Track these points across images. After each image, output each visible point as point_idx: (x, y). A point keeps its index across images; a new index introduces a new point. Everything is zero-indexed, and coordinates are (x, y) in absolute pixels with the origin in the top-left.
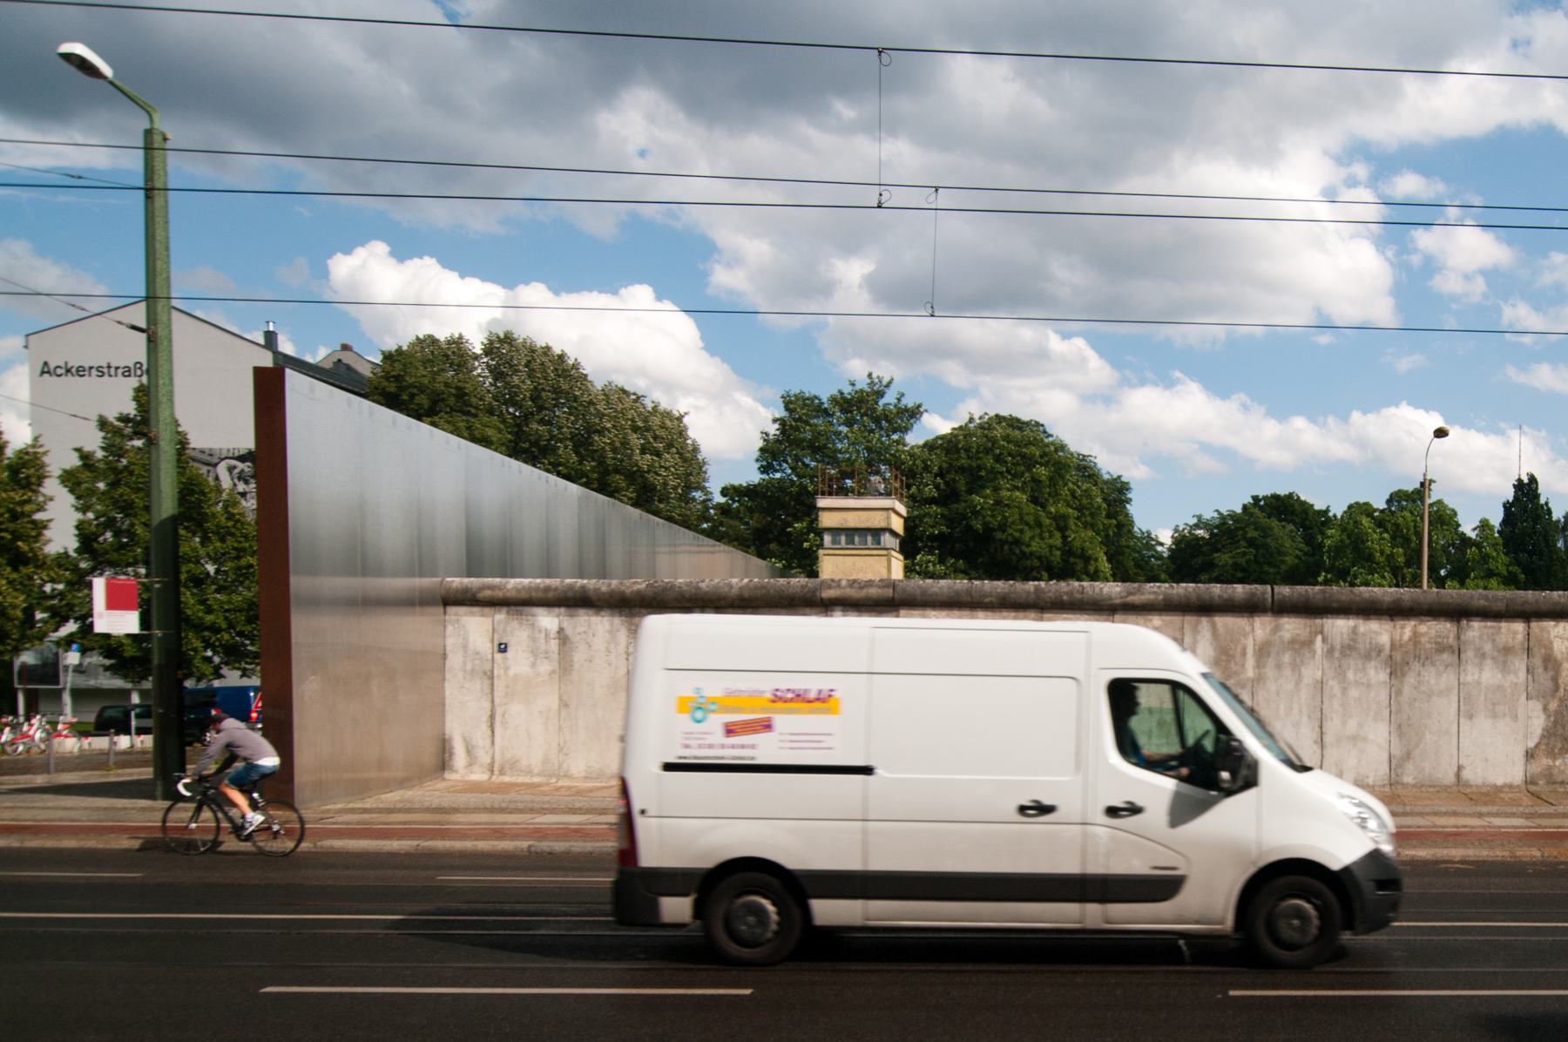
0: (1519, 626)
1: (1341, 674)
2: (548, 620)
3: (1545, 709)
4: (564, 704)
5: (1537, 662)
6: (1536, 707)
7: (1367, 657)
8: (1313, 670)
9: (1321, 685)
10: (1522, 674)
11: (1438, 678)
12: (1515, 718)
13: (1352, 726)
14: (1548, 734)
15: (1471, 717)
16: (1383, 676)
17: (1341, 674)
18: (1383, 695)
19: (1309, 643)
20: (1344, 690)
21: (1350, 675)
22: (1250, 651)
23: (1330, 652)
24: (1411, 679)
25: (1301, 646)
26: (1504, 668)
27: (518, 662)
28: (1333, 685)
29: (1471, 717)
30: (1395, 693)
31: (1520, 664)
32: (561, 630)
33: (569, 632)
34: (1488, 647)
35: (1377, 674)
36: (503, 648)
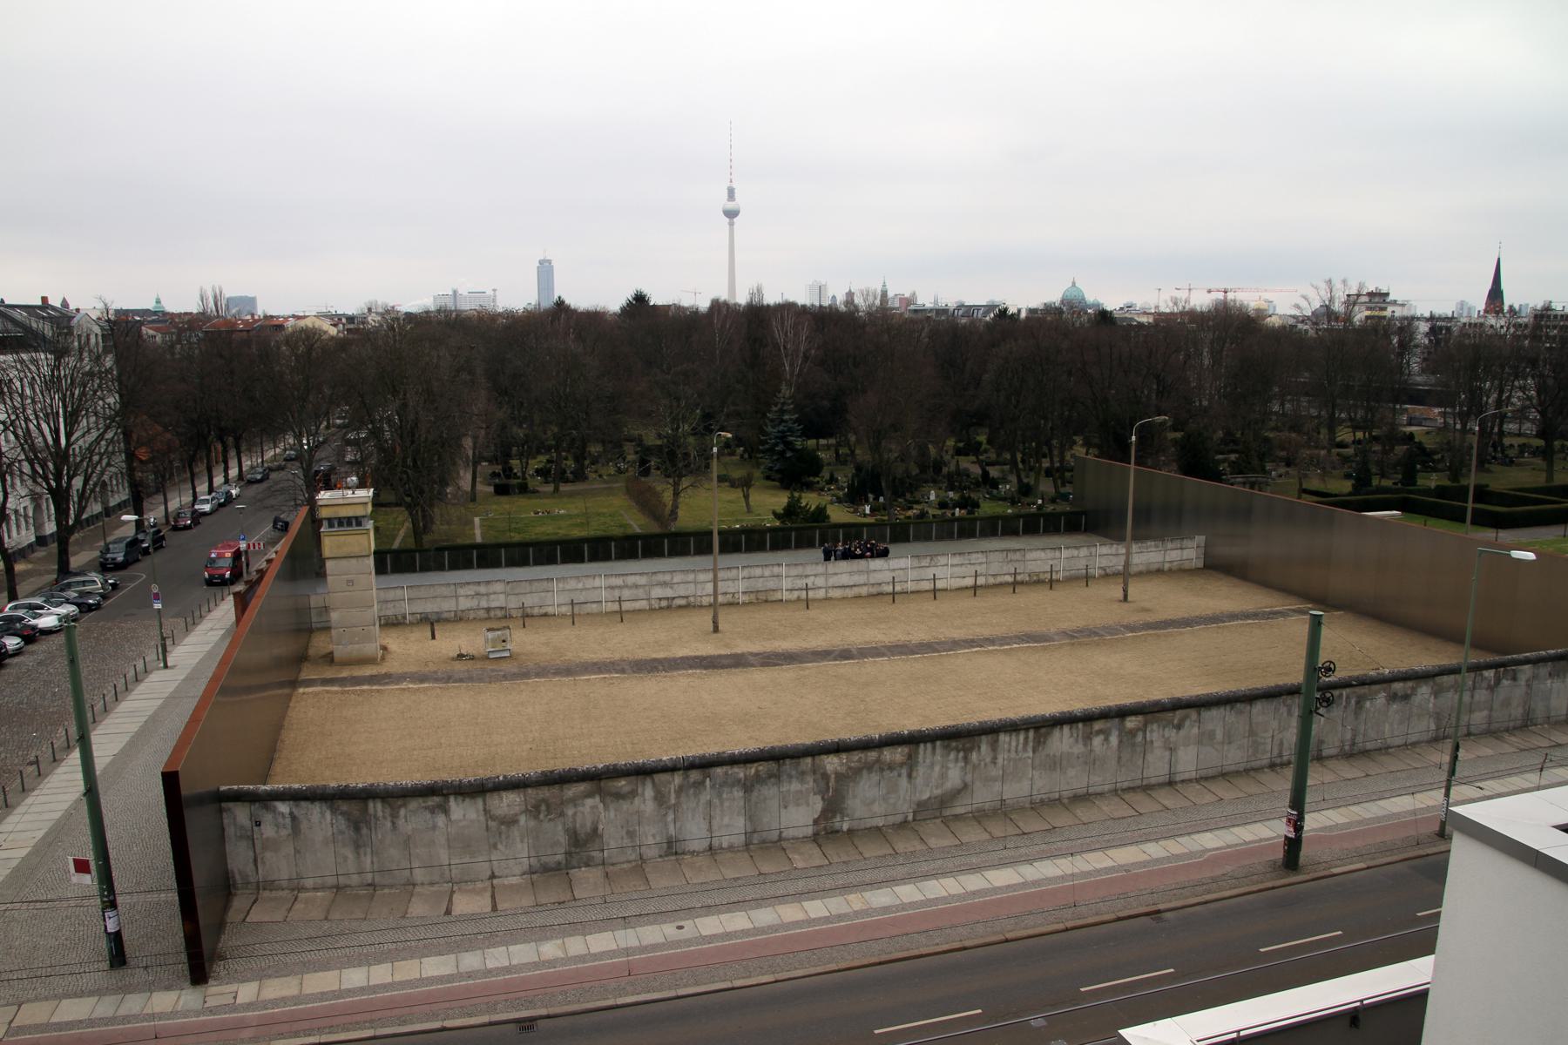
0: (809, 760)
1: (720, 795)
2: (283, 807)
4: (297, 851)
5: (818, 776)
7: (733, 785)
8: (706, 796)
9: (710, 803)
11: (769, 791)
13: (726, 820)
14: (824, 811)
16: (741, 794)
17: (720, 795)
19: (703, 782)
23: (713, 787)
24: (755, 794)
25: (699, 785)
26: (802, 781)
27: (268, 830)
28: (716, 801)
30: (747, 800)
31: (810, 779)
32: (291, 813)
33: (296, 812)
35: (738, 793)
36: (258, 824)
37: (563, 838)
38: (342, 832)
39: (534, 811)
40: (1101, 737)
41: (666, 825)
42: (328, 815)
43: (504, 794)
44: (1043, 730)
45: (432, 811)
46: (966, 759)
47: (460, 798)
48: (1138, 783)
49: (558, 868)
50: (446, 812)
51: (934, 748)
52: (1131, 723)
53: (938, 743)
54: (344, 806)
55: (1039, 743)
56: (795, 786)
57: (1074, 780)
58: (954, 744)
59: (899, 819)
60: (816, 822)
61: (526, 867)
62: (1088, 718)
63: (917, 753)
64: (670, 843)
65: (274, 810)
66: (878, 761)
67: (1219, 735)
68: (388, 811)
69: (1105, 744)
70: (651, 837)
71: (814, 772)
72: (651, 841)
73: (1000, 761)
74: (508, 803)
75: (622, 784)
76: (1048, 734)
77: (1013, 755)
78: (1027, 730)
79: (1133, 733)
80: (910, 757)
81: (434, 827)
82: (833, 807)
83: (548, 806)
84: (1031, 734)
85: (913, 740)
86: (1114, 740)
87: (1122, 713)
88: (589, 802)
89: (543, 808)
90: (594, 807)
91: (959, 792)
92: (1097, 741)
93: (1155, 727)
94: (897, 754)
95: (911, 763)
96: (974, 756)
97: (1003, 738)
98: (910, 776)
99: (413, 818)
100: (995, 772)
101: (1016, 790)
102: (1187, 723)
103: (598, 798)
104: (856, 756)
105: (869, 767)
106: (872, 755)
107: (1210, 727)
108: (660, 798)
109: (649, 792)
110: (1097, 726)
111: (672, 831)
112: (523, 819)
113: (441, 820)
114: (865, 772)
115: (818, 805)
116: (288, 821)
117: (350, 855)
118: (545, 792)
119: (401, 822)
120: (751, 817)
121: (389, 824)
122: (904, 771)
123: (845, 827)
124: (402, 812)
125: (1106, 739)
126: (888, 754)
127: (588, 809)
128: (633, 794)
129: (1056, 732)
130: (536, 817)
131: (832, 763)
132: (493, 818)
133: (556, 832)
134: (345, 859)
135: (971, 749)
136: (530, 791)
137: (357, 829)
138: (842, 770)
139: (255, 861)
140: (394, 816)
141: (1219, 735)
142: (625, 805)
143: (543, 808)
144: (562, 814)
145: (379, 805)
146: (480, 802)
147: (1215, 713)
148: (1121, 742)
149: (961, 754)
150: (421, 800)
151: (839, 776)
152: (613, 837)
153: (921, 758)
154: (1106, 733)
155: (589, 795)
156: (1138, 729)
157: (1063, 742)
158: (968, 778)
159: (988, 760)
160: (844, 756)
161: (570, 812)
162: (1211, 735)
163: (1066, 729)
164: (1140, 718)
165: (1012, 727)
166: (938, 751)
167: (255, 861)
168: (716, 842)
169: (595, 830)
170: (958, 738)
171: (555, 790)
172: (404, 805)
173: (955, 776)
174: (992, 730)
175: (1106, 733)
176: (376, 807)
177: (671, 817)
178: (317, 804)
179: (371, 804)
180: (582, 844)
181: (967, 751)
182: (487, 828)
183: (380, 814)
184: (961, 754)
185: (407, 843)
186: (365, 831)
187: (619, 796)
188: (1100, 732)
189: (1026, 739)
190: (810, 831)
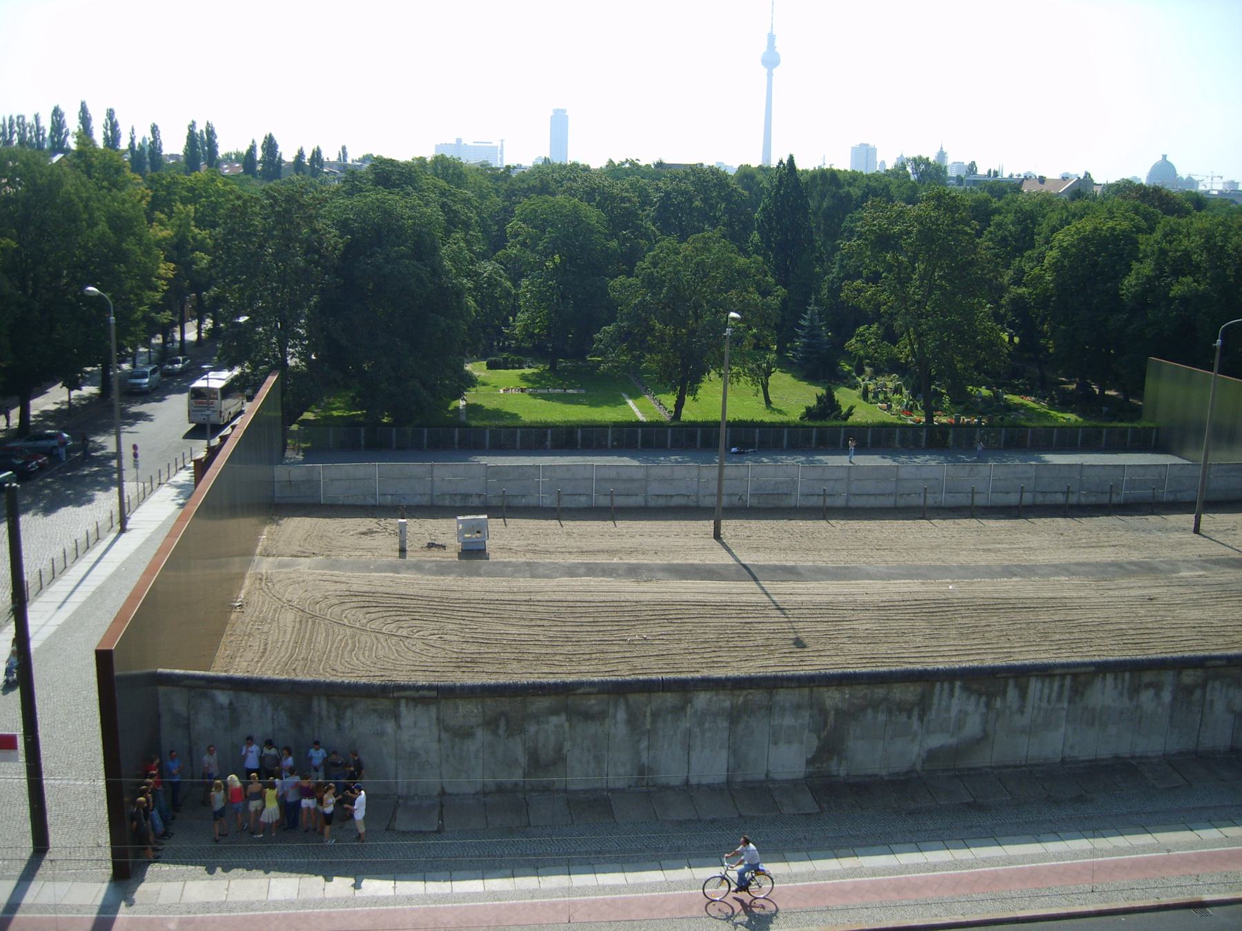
2: (223, 697)
3: (819, 737)
8: (685, 724)
9: (689, 733)
10: (807, 719)
15: (776, 744)
16: (726, 724)
18: (726, 734)
19: (683, 708)
21: (707, 725)
22: (648, 714)
25: (679, 710)
28: (697, 730)
29: (776, 744)
31: (806, 715)
32: (231, 704)
37: (523, 759)
39: (491, 724)
42: (269, 709)
43: (460, 702)
46: (988, 705)
50: (397, 717)
51: (952, 690)
52: (1188, 677)
53: (958, 684)
56: (788, 721)
58: (975, 686)
60: (809, 762)
65: (213, 699)
66: (885, 699)
71: (811, 707)
73: (1028, 710)
77: (1044, 704)
78: (1063, 676)
79: (1189, 690)
81: (381, 734)
83: (508, 722)
86: (1167, 696)
88: (554, 720)
89: (502, 723)
92: (1146, 696)
93: (1217, 684)
94: (910, 693)
95: (923, 705)
96: (998, 703)
97: (1034, 686)
98: (921, 719)
103: (563, 717)
104: (862, 691)
105: (875, 705)
106: (880, 692)
108: (633, 721)
109: (621, 715)
110: (1148, 677)
111: (644, 758)
112: (479, 733)
113: (389, 726)
114: (870, 711)
115: (812, 743)
118: (505, 705)
119: (347, 724)
120: (734, 751)
121: (334, 726)
122: (915, 713)
123: (843, 773)
124: (349, 713)
125: (1157, 695)
126: (900, 693)
129: (1098, 683)
131: (832, 698)
132: (446, 729)
140: (340, 717)
142: (593, 728)
143: (502, 723)
144: (522, 731)
145: (324, 703)
146: (433, 711)
148: (1174, 699)
149: (984, 699)
150: (369, 701)
151: (838, 712)
153: (935, 700)
154: (1157, 687)
155: (554, 712)
159: (1015, 707)
161: (532, 729)
163: (1110, 678)
164: (1200, 672)
165: (1044, 671)
166: (957, 692)
169: (559, 749)
173: (973, 727)
174: (1021, 674)
175: (1157, 687)
177: (644, 744)
181: (990, 696)
182: (440, 740)
183: (324, 713)
184: (984, 699)
187: (588, 716)
188: (1148, 686)
189: (1061, 686)
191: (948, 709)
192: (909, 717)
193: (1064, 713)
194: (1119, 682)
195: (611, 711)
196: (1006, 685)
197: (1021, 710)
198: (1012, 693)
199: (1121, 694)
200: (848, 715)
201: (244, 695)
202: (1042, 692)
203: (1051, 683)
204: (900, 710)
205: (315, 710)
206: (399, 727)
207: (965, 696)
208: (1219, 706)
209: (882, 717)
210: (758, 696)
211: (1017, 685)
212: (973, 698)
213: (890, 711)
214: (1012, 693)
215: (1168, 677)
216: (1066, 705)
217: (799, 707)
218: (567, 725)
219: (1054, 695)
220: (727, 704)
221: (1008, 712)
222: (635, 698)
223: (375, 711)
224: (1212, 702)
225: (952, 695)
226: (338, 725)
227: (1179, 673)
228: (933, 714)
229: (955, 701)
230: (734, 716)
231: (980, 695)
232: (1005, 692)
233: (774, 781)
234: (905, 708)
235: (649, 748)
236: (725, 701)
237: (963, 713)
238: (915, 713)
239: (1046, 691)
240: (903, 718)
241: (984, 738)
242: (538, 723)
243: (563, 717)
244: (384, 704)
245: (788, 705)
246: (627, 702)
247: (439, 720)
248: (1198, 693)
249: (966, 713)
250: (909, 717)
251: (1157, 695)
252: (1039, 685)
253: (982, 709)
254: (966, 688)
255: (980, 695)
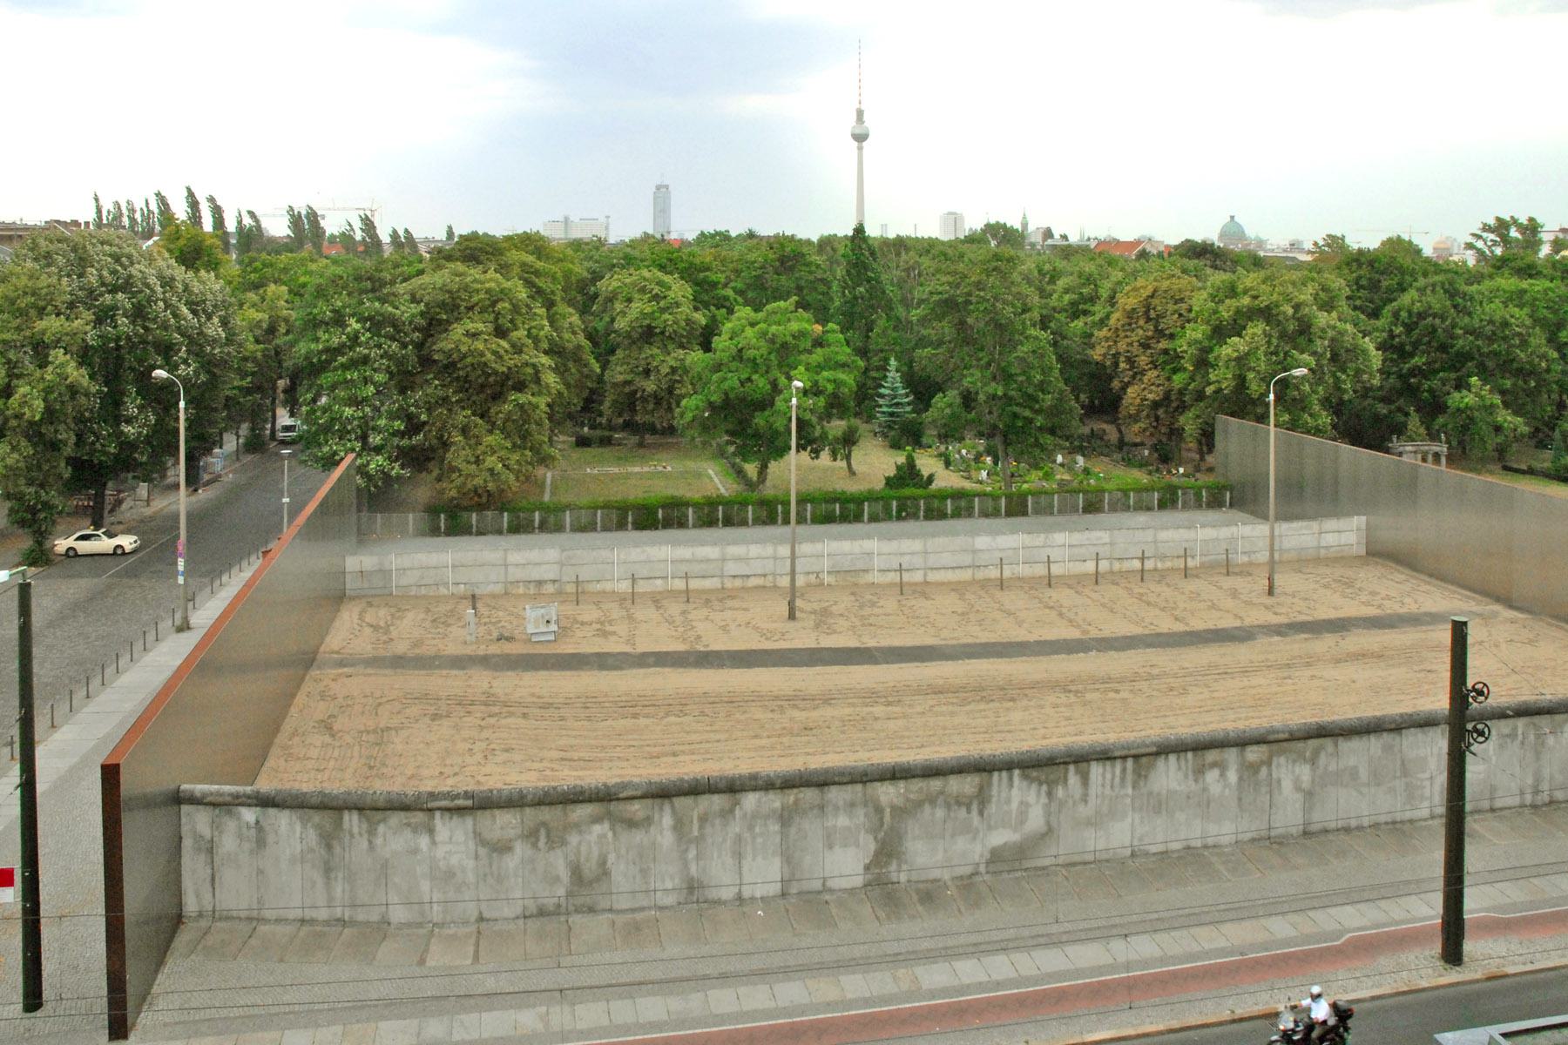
5: (871, 810)
6: (871, 838)
7: (767, 817)
8: (735, 827)
9: (739, 839)
10: (862, 818)
11: (811, 827)
12: (858, 846)
14: (877, 854)
16: (777, 827)
17: (751, 828)
19: (732, 811)
20: (754, 838)
21: (757, 830)
24: (793, 830)
25: (727, 814)
28: (747, 835)
30: (784, 835)
32: (257, 822)
34: (841, 803)
38: (311, 850)
39: (531, 836)
40: (1215, 773)
41: (686, 865)
42: (298, 828)
43: (497, 812)
44: (1144, 760)
45: (415, 830)
46: (1049, 794)
47: (447, 815)
48: (1264, 833)
49: (557, 911)
50: (431, 831)
51: (1011, 779)
52: (1253, 754)
53: (1017, 772)
54: (317, 817)
55: (1140, 775)
56: (842, 821)
57: (1188, 829)
59: (968, 870)
60: (867, 868)
61: (519, 911)
62: (1199, 746)
63: (990, 784)
64: (691, 889)
66: (942, 793)
67: (1363, 774)
68: (365, 826)
69: (1222, 781)
70: (667, 882)
71: (866, 805)
72: (669, 885)
74: (505, 823)
75: (637, 809)
76: (1151, 766)
77: (1108, 791)
78: (1124, 758)
79: (1253, 768)
80: (981, 789)
81: (415, 851)
82: (888, 850)
84: (1130, 762)
85: (983, 768)
86: (1232, 776)
87: (1242, 742)
89: (543, 832)
90: (602, 836)
91: (1043, 836)
92: (1212, 776)
93: (1282, 760)
94: (965, 785)
96: (1060, 792)
97: (1096, 769)
98: (981, 813)
99: (394, 837)
100: (1085, 811)
101: (1120, 835)
102: (1323, 756)
103: (606, 825)
104: (917, 785)
105: (932, 801)
106: (936, 784)
107: (1352, 762)
108: (679, 826)
109: (667, 820)
110: (1211, 756)
113: (424, 841)
114: (927, 807)
116: (253, 832)
117: (320, 881)
118: (546, 814)
119: (379, 841)
120: (788, 859)
121: (365, 844)
122: (975, 807)
124: (381, 828)
125: (1222, 775)
126: (955, 785)
127: (593, 837)
128: (648, 821)
129: (1160, 762)
130: (535, 845)
131: (888, 793)
133: (559, 862)
134: (314, 884)
135: (1055, 782)
136: (528, 810)
137: (329, 847)
138: (899, 802)
139: (213, 879)
140: (372, 832)
141: (1363, 774)
142: (638, 836)
143: (543, 832)
144: (564, 843)
146: (469, 821)
147: (1356, 744)
148: (1241, 779)
149: (1044, 788)
151: (894, 808)
152: (622, 875)
153: (994, 792)
154: (1221, 766)
155: (597, 820)
156: (1263, 763)
157: (1169, 776)
158: (1053, 820)
160: (902, 784)
162: (1354, 773)
163: (1172, 758)
164: (1264, 748)
165: (1105, 756)
167: (213, 879)
168: (747, 892)
169: (603, 862)
170: (1042, 767)
171: (558, 811)
172: (384, 820)
173: (1036, 820)
174: (1080, 759)
175: (1221, 766)
176: (351, 820)
177: (692, 854)
178: (287, 812)
179: (346, 815)
180: (586, 883)
181: (1051, 784)
182: (477, 857)
183: (356, 830)
184: (1044, 788)
185: (384, 870)
186: (337, 850)
187: (631, 824)
188: (1214, 765)
189: (1124, 770)
190: (858, 881)
191: (1008, 801)
192: (969, 812)
193: (1128, 801)
194: (1183, 763)
195: (656, 817)
196: (1067, 771)
197: (1085, 799)
198: (1073, 779)
199: (1186, 776)
200: (900, 812)
201: (272, 811)
202: (1104, 776)
203: (1113, 767)
204: (959, 803)
205: (346, 825)
206: (434, 843)
207: (1025, 783)
208: (1287, 785)
209: (940, 813)
210: (809, 795)
211: (1077, 772)
212: (1034, 786)
213: (948, 806)
214: (1073, 779)
215: (1231, 755)
216: (1130, 791)
217: (852, 805)
218: (610, 834)
219: (1117, 780)
220: (777, 804)
221: (1071, 802)
222: (679, 802)
223: (408, 825)
224: (1279, 781)
225: (1011, 786)
226: (370, 842)
227: (1243, 751)
228: (992, 808)
229: (1015, 791)
230: (785, 818)
231: (1041, 784)
232: (1066, 780)
233: (831, 891)
234: (961, 802)
235: (698, 857)
236: (775, 801)
237: (1024, 805)
238: (975, 807)
239: (1109, 776)
240: (963, 812)
241: (1049, 832)
242: (580, 832)
243: (606, 825)
244: (419, 817)
245: (841, 803)
246: (673, 807)
247: (477, 835)
248: (1264, 770)
249: (1027, 805)
250: (969, 812)
251: (1222, 775)
252: (1100, 770)
253: (1044, 800)
254: (1025, 777)
255: (1041, 784)
